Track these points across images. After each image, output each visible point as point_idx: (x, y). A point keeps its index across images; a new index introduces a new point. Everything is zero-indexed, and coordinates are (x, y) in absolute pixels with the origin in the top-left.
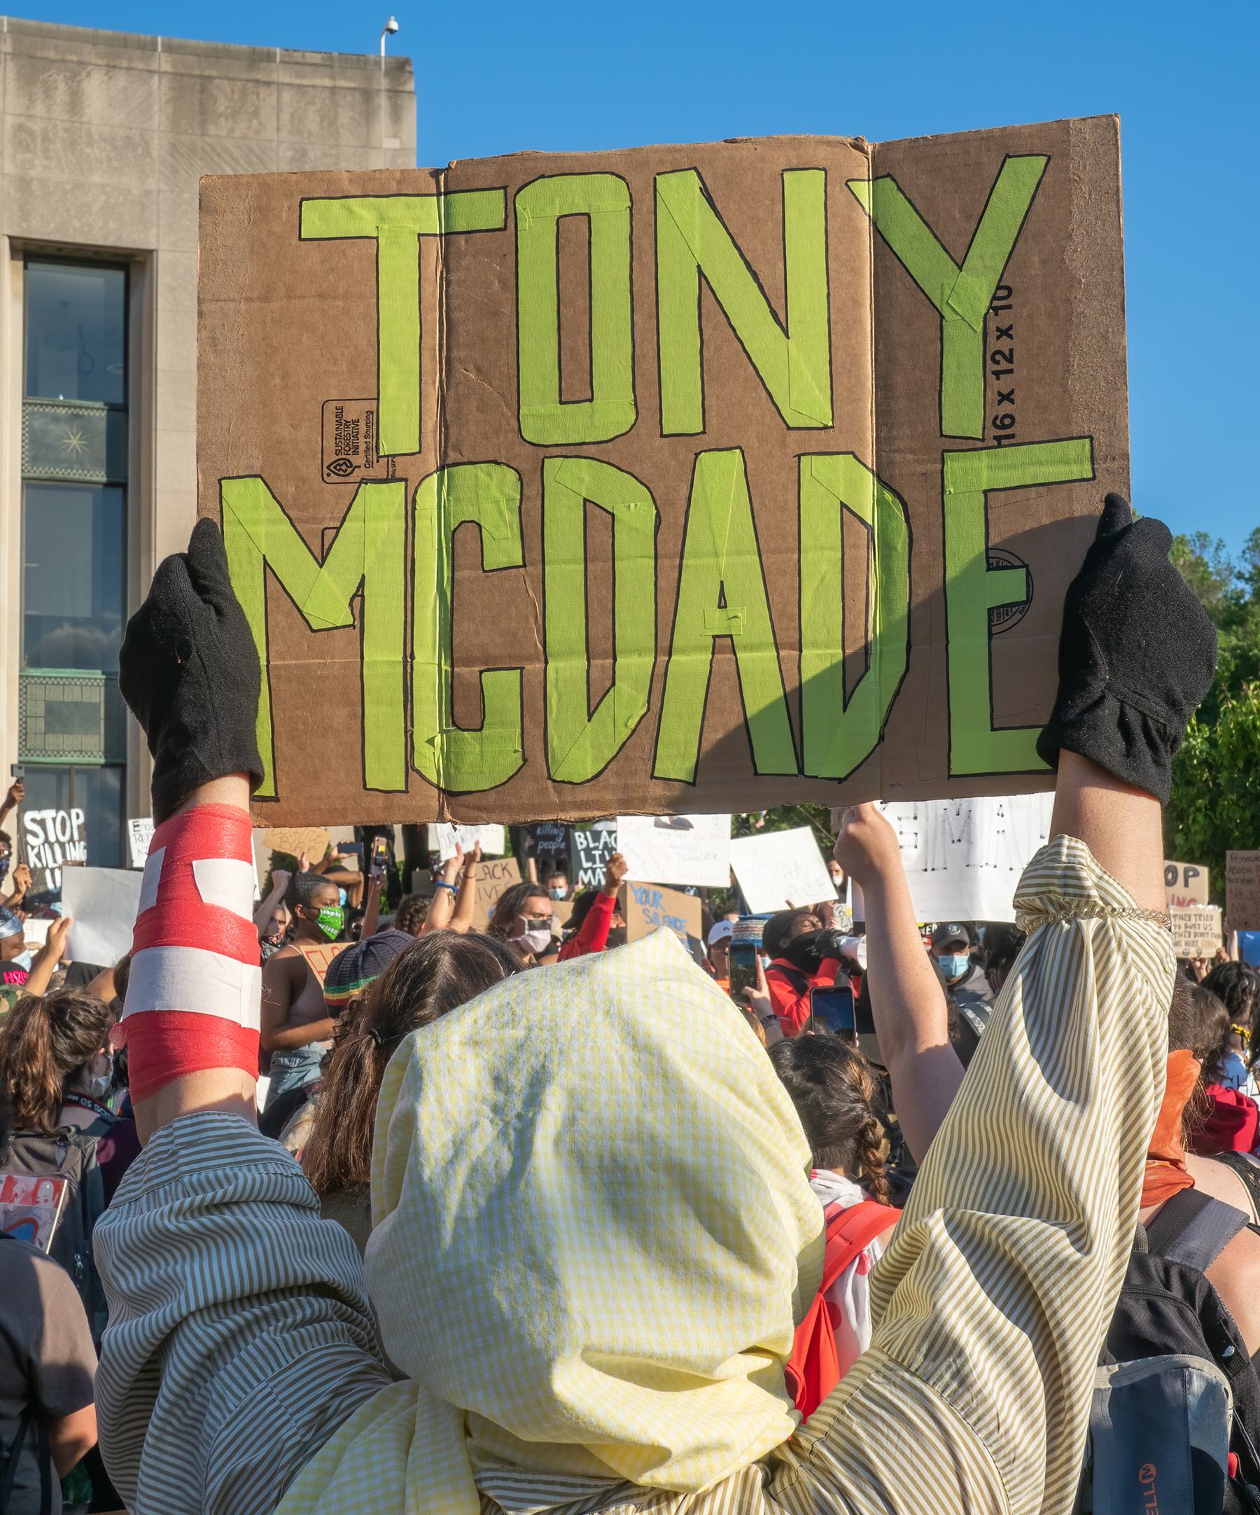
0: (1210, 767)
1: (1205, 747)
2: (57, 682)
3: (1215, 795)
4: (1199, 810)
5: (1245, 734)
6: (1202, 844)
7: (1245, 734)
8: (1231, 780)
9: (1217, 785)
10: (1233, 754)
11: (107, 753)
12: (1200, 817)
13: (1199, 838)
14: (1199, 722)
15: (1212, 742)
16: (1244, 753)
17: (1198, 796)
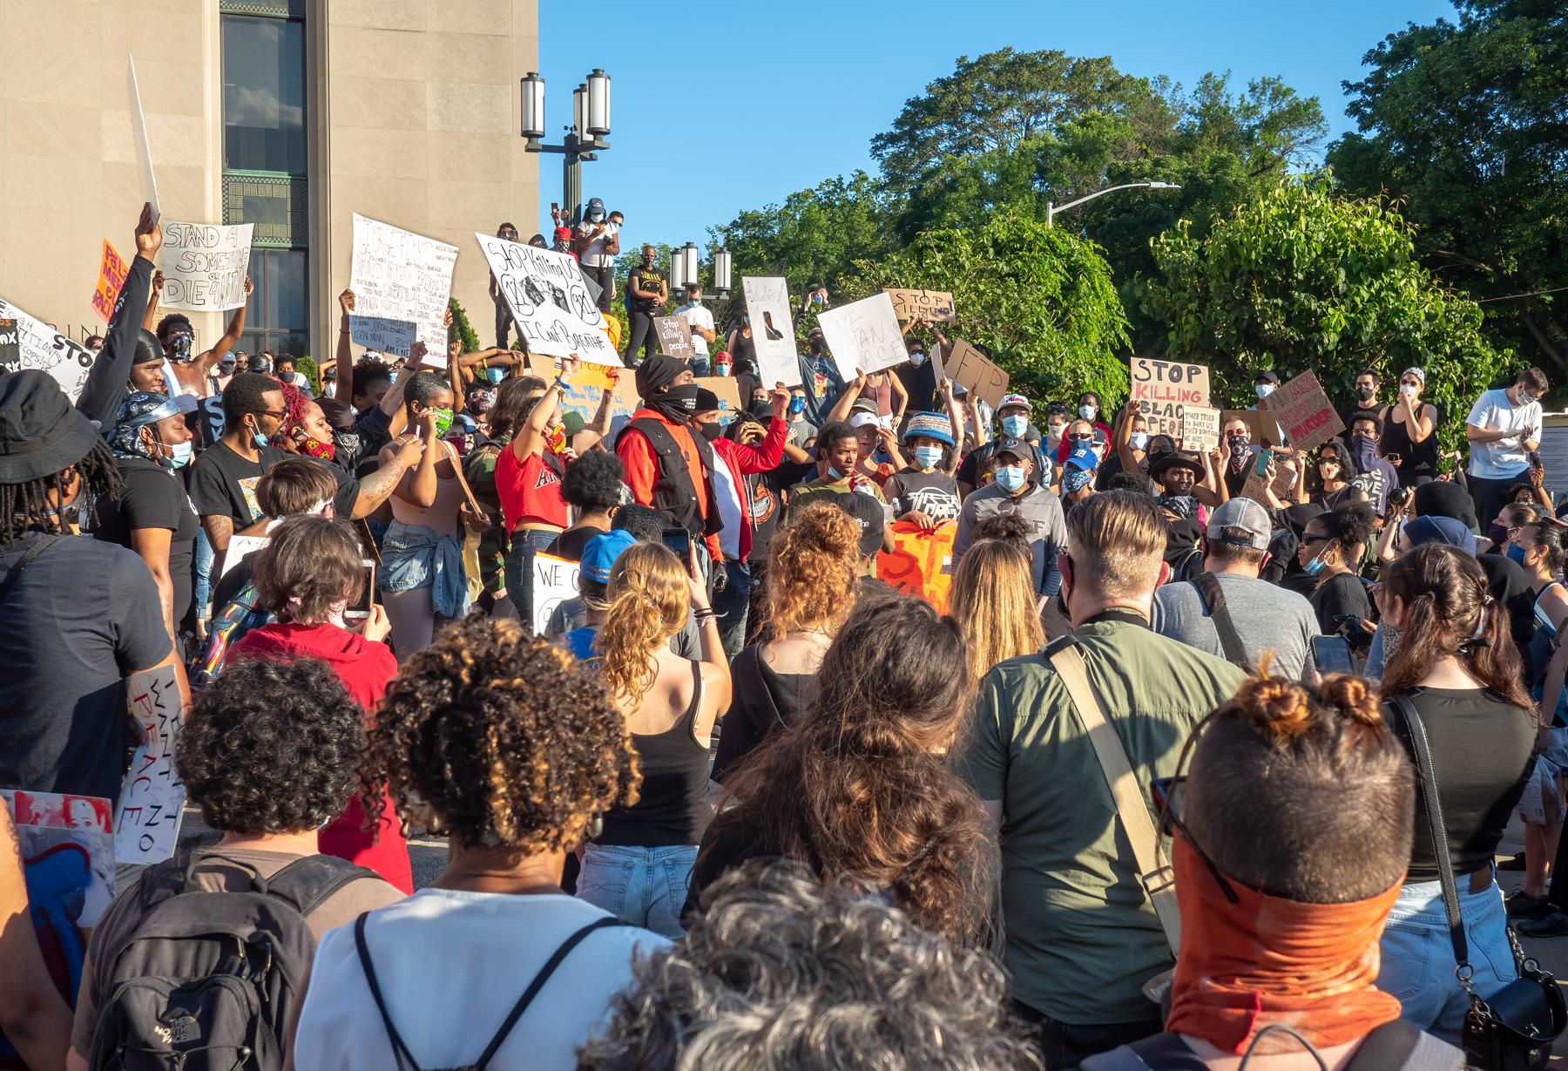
0: (1200, 276)
1: (1196, 257)
2: (259, 182)
3: (1205, 300)
4: (1190, 312)
5: (1233, 249)
6: (1192, 341)
7: (1233, 249)
8: (1220, 287)
9: (1206, 290)
10: (1221, 263)
11: (293, 239)
12: (1192, 319)
13: (1190, 336)
14: (1190, 237)
15: (1200, 252)
16: (1231, 265)
17: (1190, 300)
